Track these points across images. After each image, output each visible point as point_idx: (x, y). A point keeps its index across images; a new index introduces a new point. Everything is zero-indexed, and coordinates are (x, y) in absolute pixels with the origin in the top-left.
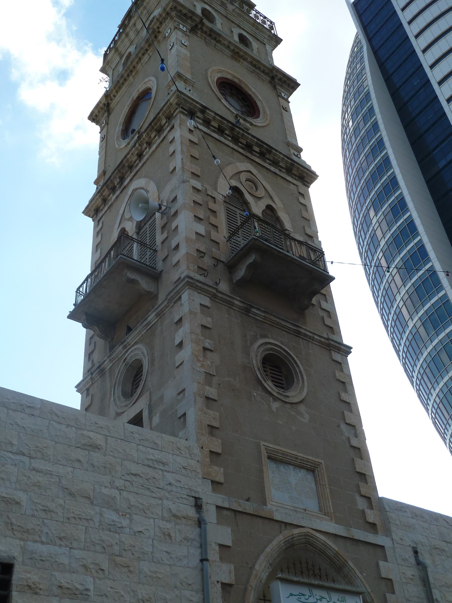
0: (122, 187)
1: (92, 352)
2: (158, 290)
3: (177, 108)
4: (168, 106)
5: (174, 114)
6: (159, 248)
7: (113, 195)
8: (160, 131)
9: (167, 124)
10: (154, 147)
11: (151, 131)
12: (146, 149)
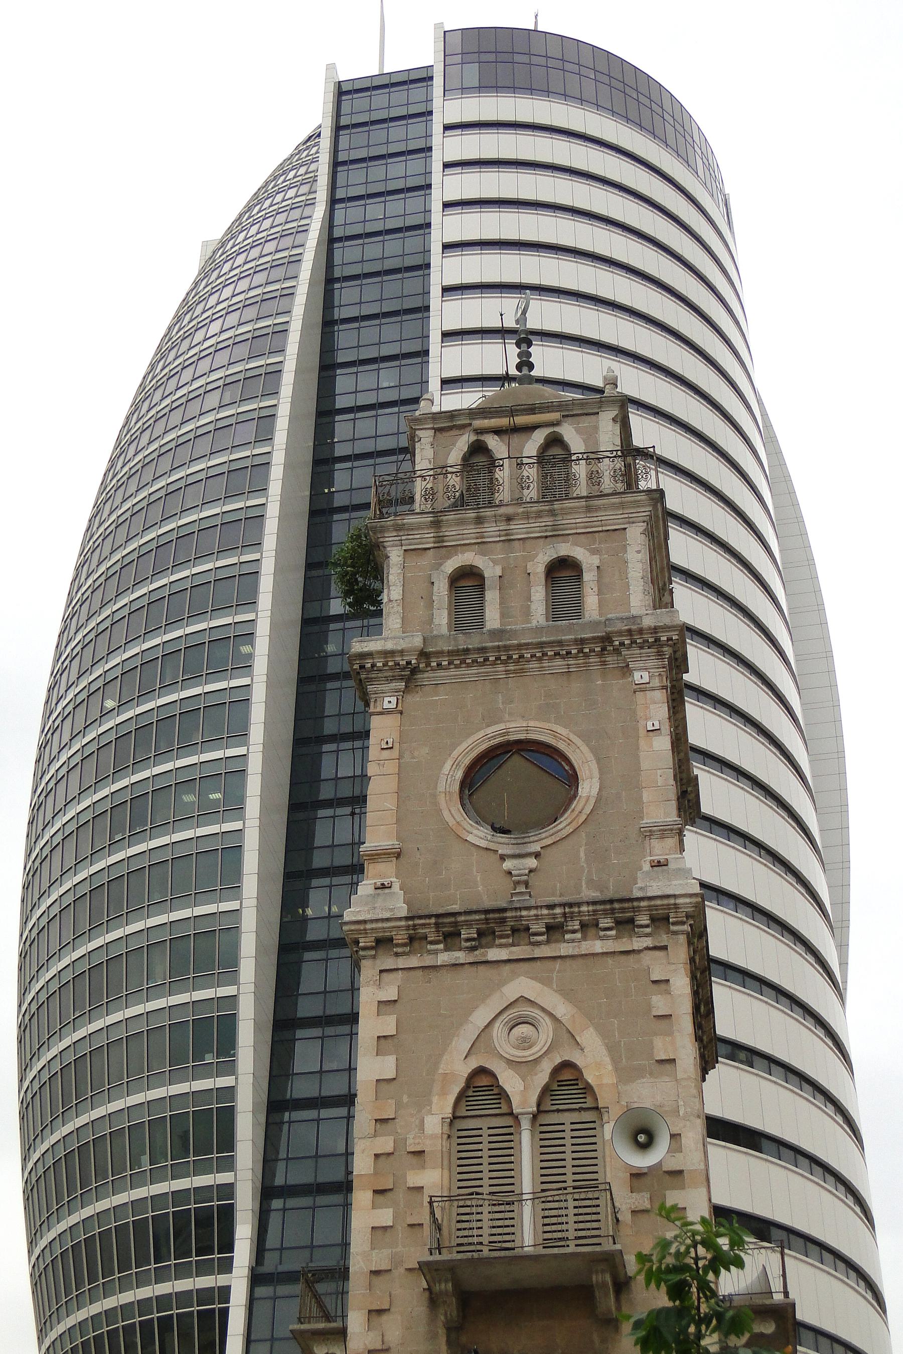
0: (478, 955)
1: (380, 1312)
2: (619, 1308)
3: (683, 923)
4: (669, 905)
5: (673, 928)
6: (625, 1217)
7: (447, 949)
8: (626, 924)
9: (648, 930)
10: (598, 946)
11: (605, 913)
12: (574, 932)
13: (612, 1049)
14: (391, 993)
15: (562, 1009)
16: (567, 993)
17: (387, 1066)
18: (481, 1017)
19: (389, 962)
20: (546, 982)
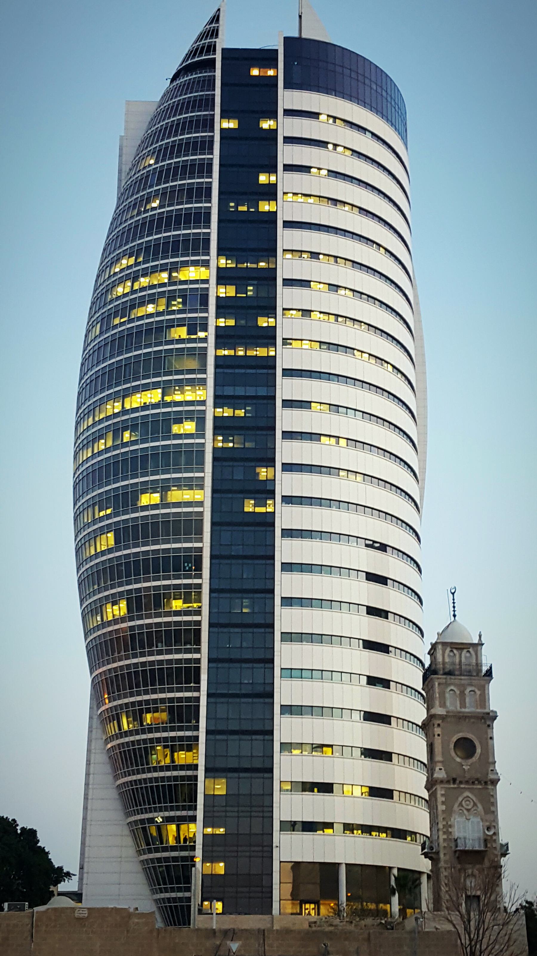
13: (484, 808)
14: (443, 792)
15: (474, 799)
16: (475, 796)
17: (444, 807)
18: (460, 799)
19: (442, 786)
20: (471, 792)
